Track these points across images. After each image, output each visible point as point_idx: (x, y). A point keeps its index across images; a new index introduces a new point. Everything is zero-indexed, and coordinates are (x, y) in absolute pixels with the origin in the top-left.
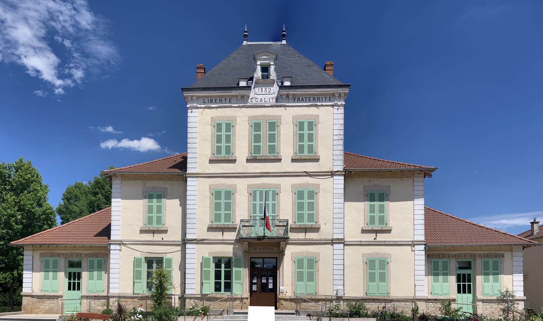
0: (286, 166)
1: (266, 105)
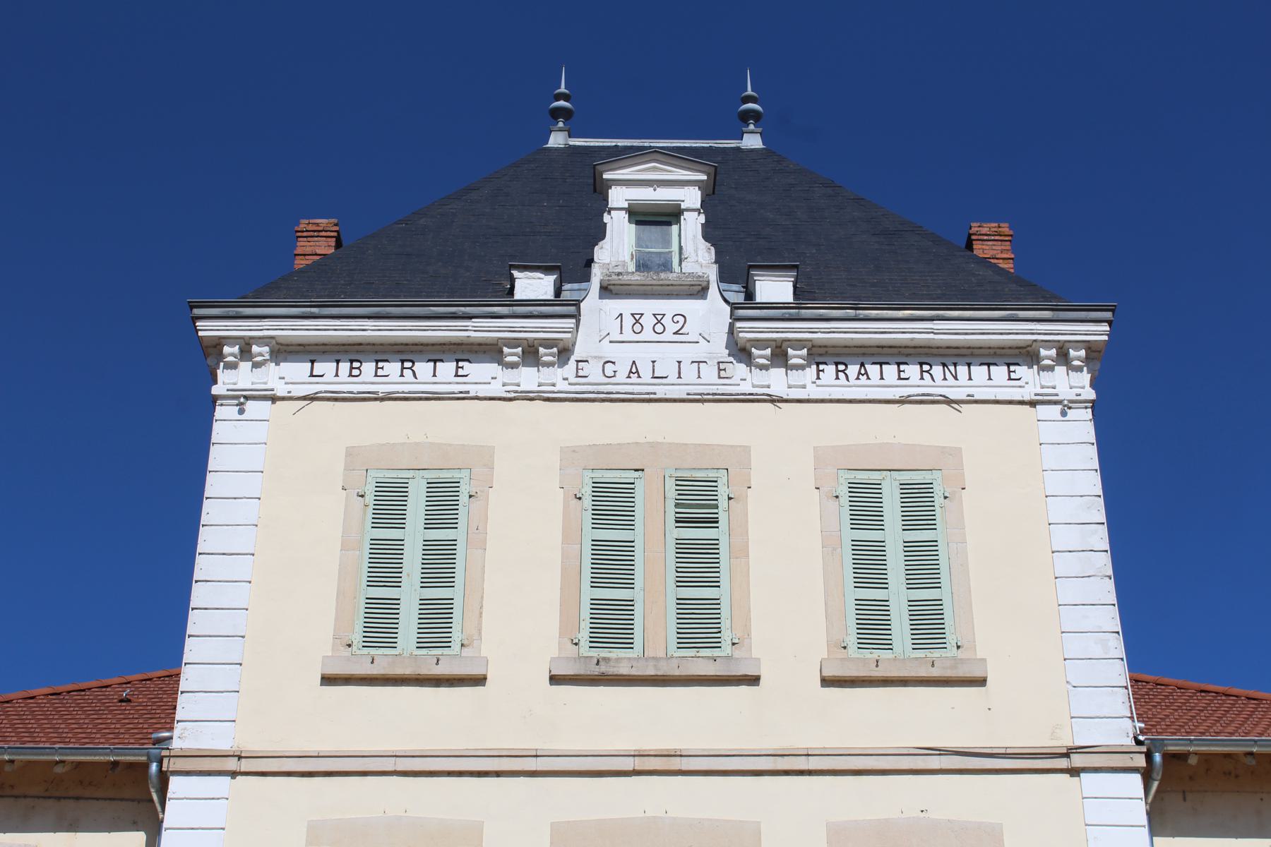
0: (790, 710)
1: (661, 392)
